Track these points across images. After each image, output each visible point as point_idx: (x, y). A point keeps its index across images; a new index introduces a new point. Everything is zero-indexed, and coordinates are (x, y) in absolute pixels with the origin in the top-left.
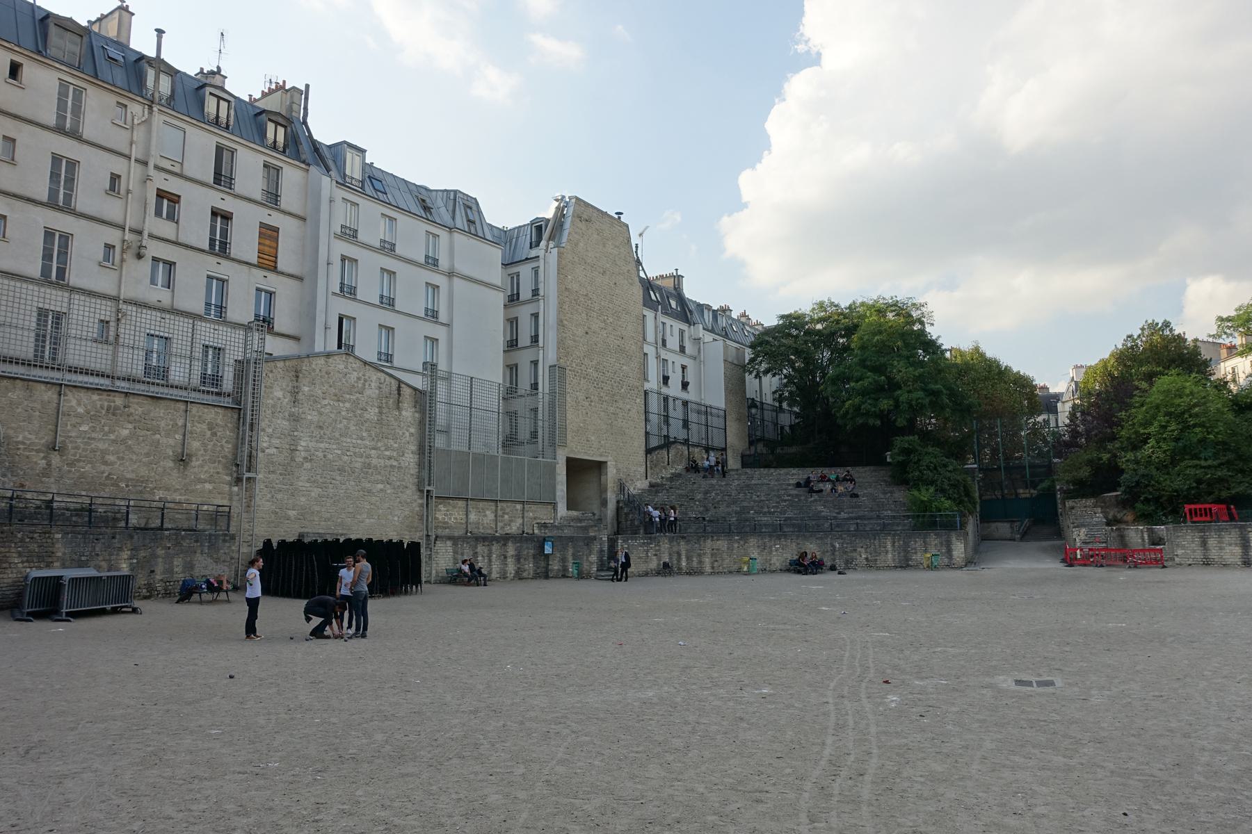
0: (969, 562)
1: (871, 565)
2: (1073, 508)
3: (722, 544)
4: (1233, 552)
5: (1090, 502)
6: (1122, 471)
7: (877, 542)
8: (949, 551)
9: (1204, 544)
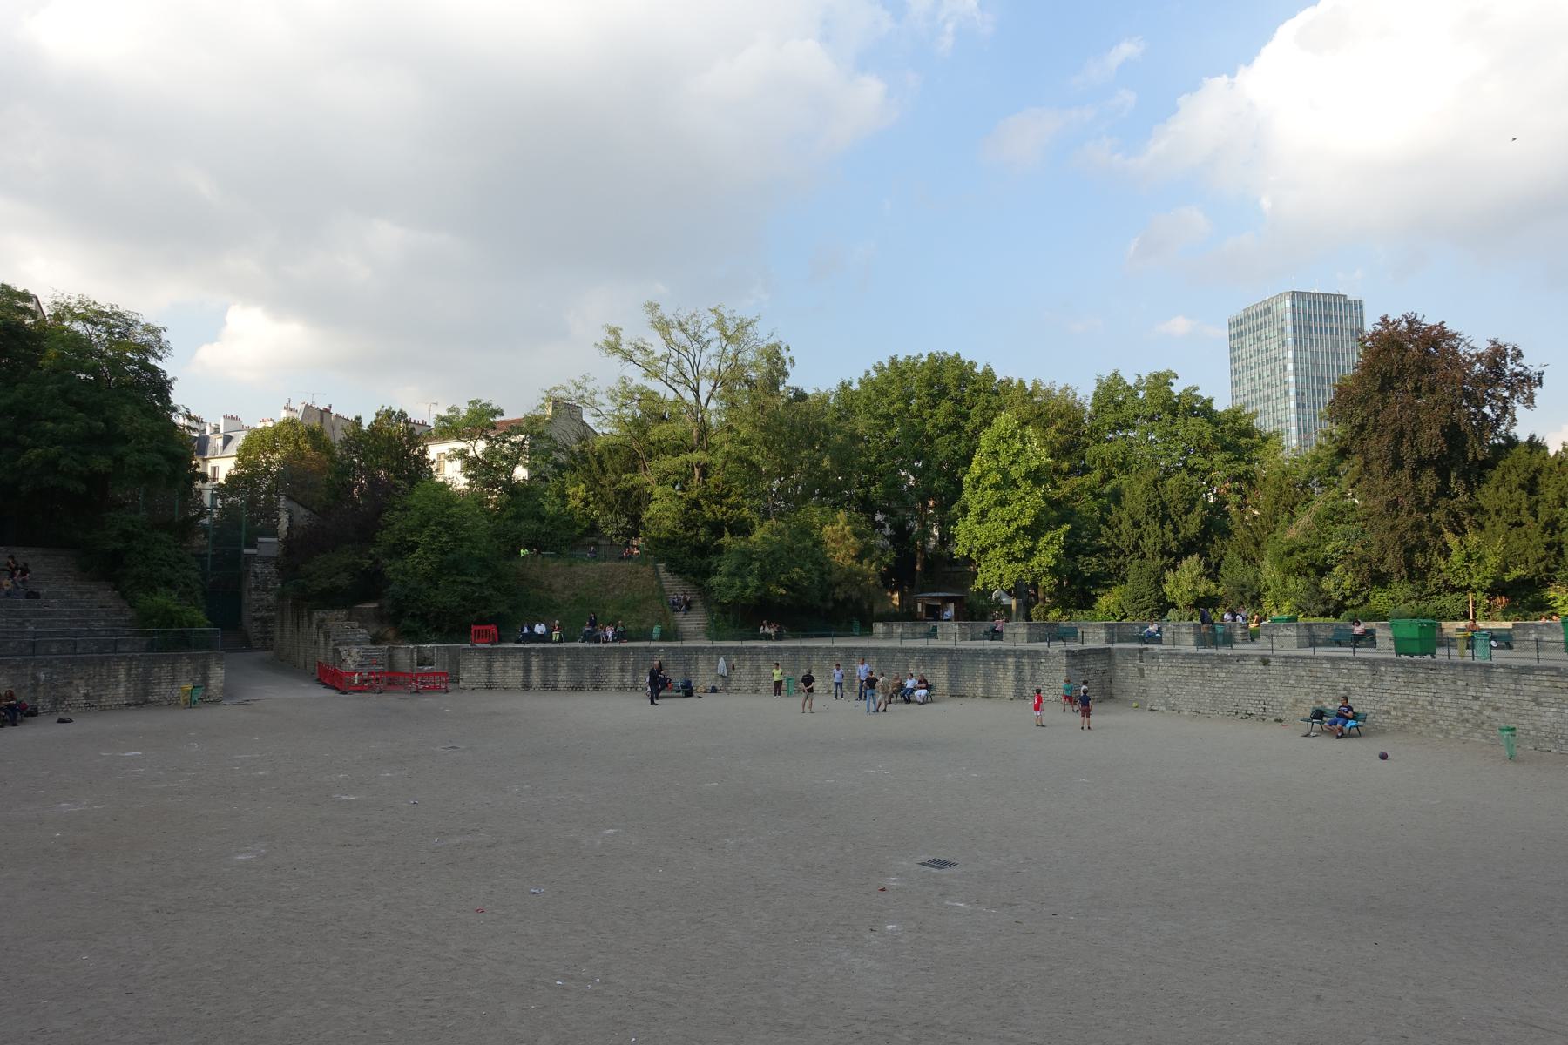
0: (228, 693)
1: (93, 705)
2: (323, 620)
4: (515, 676)
5: (343, 613)
6: (390, 582)
7: (104, 671)
8: (205, 679)
9: (489, 667)
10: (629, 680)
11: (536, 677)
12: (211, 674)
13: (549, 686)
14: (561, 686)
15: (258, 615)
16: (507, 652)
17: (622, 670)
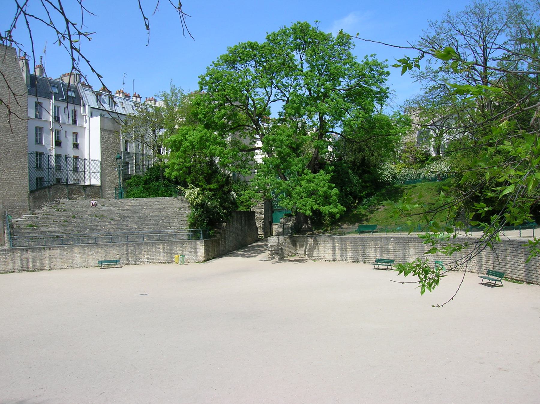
3: (57, 252)
4: (329, 254)
7: (154, 248)
8: (196, 252)
12: (198, 250)
13: (344, 259)
14: (349, 259)
17: (375, 251)
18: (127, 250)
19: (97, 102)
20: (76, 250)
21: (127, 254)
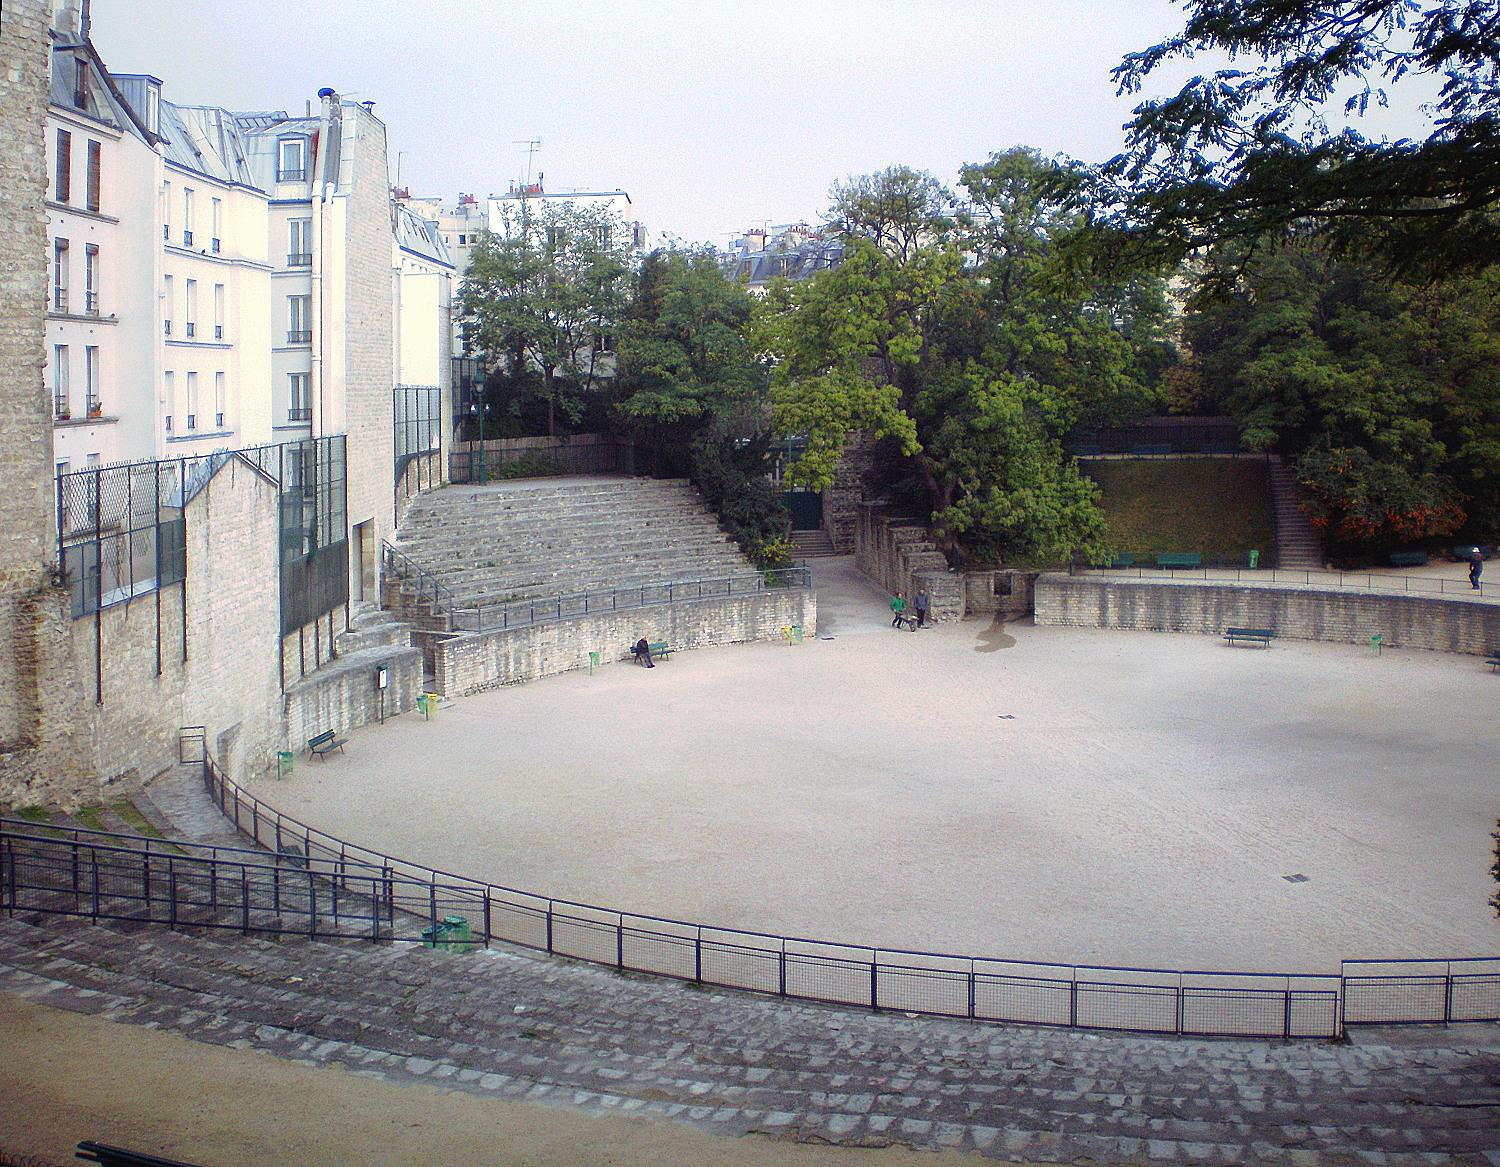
3: (553, 634)
4: (1092, 612)
7: (722, 612)
8: (801, 616)
9: (1064, 603)
10: (1211, 622)
11: (1112, 614)
13: (1126, 624)
15: (838, 516)
16: (1082, 586)
17: (1205, 611)
18: (674, 620)
19: (152, 144)
20: (586, 626)
21: (674, 628)
